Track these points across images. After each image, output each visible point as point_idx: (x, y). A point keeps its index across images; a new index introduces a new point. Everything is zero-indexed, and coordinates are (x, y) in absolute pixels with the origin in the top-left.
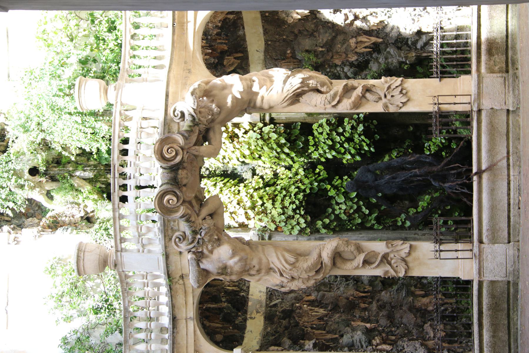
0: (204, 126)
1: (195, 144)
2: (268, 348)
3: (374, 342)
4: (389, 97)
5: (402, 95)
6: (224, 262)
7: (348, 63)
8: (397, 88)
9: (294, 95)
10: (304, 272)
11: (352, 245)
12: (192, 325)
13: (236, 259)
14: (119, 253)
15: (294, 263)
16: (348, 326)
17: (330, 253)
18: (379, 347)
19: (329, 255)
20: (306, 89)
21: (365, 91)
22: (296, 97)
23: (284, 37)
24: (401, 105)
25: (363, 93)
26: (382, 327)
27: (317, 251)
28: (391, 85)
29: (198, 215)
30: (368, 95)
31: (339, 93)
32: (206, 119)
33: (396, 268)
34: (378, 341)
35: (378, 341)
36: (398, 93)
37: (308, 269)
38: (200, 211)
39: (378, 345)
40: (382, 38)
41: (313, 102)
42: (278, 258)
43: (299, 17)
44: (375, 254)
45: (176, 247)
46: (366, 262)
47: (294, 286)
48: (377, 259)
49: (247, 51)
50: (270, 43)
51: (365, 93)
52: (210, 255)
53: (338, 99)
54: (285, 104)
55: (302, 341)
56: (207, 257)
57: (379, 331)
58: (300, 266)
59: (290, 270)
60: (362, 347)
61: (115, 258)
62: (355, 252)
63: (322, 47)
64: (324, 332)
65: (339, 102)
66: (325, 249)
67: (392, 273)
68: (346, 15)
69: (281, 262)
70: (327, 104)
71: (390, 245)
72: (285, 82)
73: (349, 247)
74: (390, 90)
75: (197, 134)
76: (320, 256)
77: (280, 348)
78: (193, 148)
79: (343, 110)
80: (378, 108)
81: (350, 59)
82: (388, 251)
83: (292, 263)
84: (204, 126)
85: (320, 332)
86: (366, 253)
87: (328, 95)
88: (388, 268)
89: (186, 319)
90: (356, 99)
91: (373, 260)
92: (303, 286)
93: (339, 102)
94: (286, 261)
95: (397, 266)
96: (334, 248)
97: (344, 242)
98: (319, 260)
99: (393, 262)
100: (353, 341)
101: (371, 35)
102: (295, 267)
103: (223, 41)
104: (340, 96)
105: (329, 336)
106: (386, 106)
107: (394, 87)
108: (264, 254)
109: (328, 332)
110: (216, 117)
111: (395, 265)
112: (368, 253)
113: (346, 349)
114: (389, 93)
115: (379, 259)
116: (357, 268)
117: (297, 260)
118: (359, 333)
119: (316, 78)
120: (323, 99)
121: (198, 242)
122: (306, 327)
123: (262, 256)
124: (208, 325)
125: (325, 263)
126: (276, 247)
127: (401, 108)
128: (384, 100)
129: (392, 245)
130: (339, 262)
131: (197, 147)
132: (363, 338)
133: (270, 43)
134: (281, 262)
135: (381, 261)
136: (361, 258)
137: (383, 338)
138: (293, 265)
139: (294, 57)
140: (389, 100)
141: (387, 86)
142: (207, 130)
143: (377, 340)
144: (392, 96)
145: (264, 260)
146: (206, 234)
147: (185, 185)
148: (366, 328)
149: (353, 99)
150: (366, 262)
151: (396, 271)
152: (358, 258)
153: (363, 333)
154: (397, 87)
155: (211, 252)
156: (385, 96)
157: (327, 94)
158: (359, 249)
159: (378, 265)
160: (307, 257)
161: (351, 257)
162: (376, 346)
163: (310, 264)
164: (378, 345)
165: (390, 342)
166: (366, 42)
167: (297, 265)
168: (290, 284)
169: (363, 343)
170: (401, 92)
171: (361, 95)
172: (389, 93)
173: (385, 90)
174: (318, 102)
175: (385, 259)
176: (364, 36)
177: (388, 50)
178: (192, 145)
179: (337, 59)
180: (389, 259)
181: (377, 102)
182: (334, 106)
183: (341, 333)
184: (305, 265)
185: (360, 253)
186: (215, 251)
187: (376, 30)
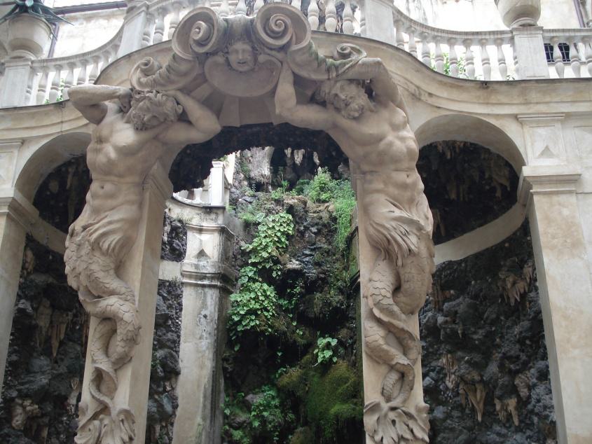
0: (327, 91)
1: (295, 75)
2: (31, 249)
3: (27, 403)
4: (392, 415)
5: (396, 440)
6: (111, 140)
7: (441, 376)
8: (409, 432)
9: (388, 241)
10: (85, 267)
11: (127, 349)
12: (54, 131)
13: (113, 155)
14: (144, 8)
15: (100, 249)
16: (70, 372)
17: (113, 308)
18: (19, 410)
19: (109, 308)
20: (400, 263)
21: (402, 369)
22: (386, 250)
23: (473, 282)
24: (378, 438)
25: (398, 366)
26: (67, 420)
27: (123, 290)
28: (416, 420)
29: (186, 91)
30: (394, 376)
31: (396, 322)
32: (338, 92)
33: (87, 429)
34: (28, 408)
35: (28, 408)
36: (400, 433)
37: (89, 273)
38: (194, 98)
39: (24, 408)
40: (482, 421)
41: (376, 276)
42: (110, 223)
43: (509, 286)
44: (112, 391)
45: (136, 66)
46: (99, 376)
47: (70, 257)
48: (104, 394)
49: (449, 240)
50: (463, 265)
51: (398, 371)
52: (124, 120)
53: (385, 318)
54: (371, 231)
55: (48, 303)
56: (123, 117)
57: (61, 415)
58: (95, 259)
59: (89, 241)
60: (23, 384)
61: (139, 5)
62: (114, 357)
63: (463, 334)
64: (62, 337)
65: (379, 321)
66: (122, 302)
67: (82, 421)
68: (518, 357)
69: (104, 226)
70: (374, 300)
71: (122, 417)
72: (411, 222)
73: (122, 344)
74: (405, 419)
75: (314, 77)
76: (112, 293)
77: (30, 268)
78: (290, 72)
79: (365, 329)
80: (371, 395)
81: (448, 378)
82: (114, 413)
83: (101, 244)
84: (327, 91)
85: (63, 331)
86: (112, 374)
87: (391, 301)
88: (90, 414)
89: (62, 122)
90: (387, 352)
91: (103, 388)
92: (67, 269)
93: (379, 321)
94: (104, 235)
95: (90, 430)
96: (121, 316)
97: (130, 334)
98: (104, 293)
99: (96, 422)
100: (35, 372)
101: (485, 404)
102: (93, 249)
103: (461, 195)
104: (389, 322)
105: (55, 344)
106: (375, 408)
107: (411, 426)
108: (122, 204)
109: (61, 343)
110: (343, 112)
111: (91, 427)
112: (111, 377)
113: (14, 358)
114: (400, 416)
115: (103, 398)
116: (94, 361)
117: (106, 254)
118: (45, 381)
119: (421, 285)
120: (383, 292)
121: (139, 93)
122: (75, 316)
123: (121, 199)
124: (70, 170)
125: (98, 302)
126: (134, 223)
127: (372, 437)
128: (385, 406)
129: (122, 421)
130: (105, 328)
131: (291, 78)
132: (35, 387)
133: (463, 265)
134: (104, 226)
135: (101, 402)
136: (105, 366)
137: (37, 417)
138: (96, 246)
139: (446, 300)
140: (386, 415)
141: (412, 411)
142: (323, 104)
143: (31, 407)
144: (394, 422)
145: (110, 203)
146: (150, 99)
147: (227, 60)
148: (66, 398)
149: (385, 347)
150: (99, 376)
151: (84, 426)
152: (106, 359)
153: (43, 387)
154: (412, 431)
155: (127, 122)
156: (393, 409)
157: (391, 299)
158: (121, 362)
159: (93, 397)
160: (112, 272)
161: (111, 350)
162: (22, 405)
163: (96, 275)
164: (24, 408)
165: (35, 427)
166: (476, 397)
167: (97, 254)
168: (74, 247)
169: (27, 386)
170: (402, 438)
171: (394, 363)
172: (400, 414)
173: (404, 409)
174: (378, 285)
175: (104, 409)
176: (484, 394)
177: (465, 431)
178: (297, 71)
179: (447, 360)
180: (101, 416)
181: (382, 393)
182: (371, 311)
183: (59, 361)
184: (94, 267)
185: (114, 363)
186: (127, 126)
187: (495, 410)
